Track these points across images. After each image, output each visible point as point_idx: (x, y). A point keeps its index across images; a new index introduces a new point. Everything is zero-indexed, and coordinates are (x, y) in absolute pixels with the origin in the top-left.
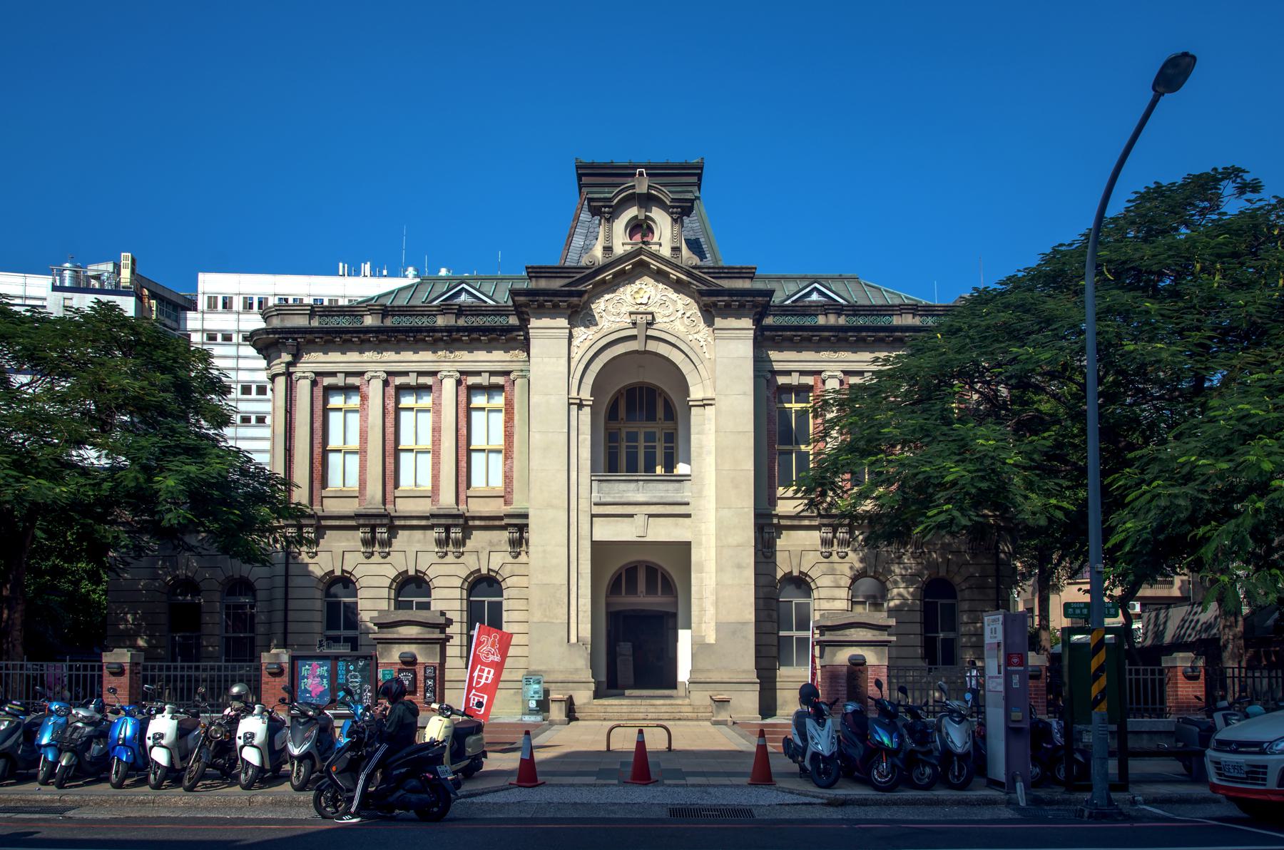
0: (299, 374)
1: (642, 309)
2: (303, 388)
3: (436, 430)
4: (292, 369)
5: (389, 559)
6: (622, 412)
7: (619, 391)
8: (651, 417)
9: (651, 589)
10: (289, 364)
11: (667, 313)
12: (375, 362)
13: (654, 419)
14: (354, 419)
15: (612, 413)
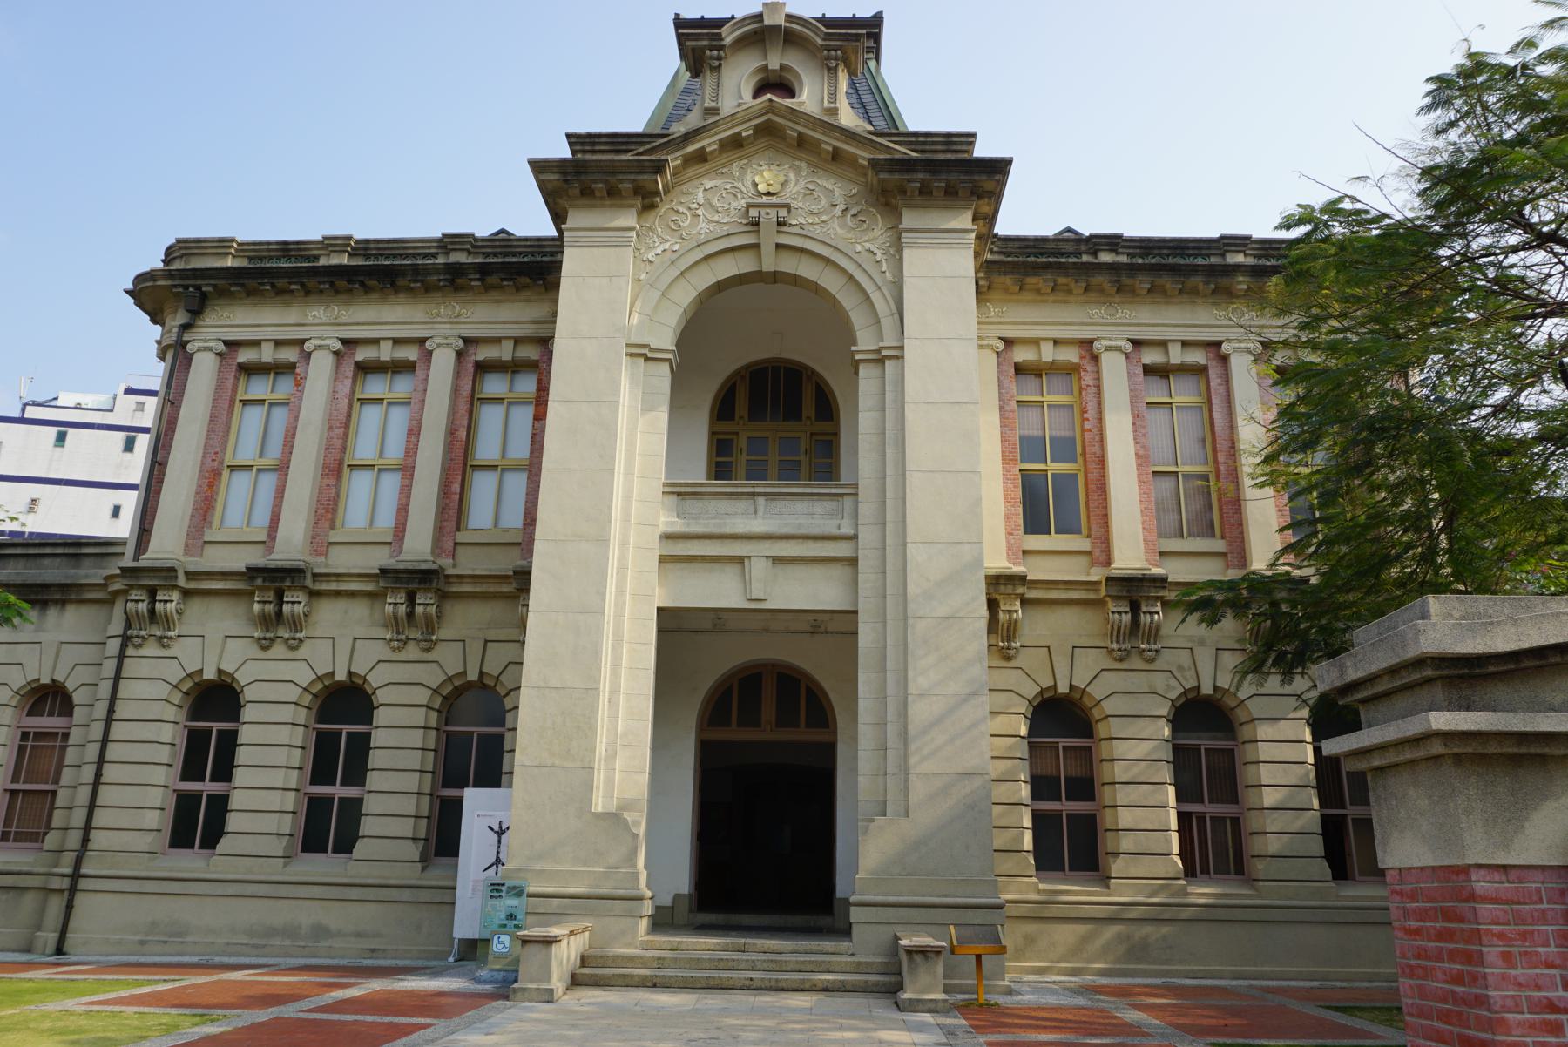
0: (197, 344)
1: (774, 200)
2: (204, 368)
3: (414, 432)
4: (186, 337)
5: (303, 652)
6: (742, 407)
7: (738, 372)
8: (793, 413)
9: (786, 717)
10: (186, 327)
11: (815, 208)
12: (321, 323)
13: (798, 417)
14: (280, 416)
15: (723, 409)
